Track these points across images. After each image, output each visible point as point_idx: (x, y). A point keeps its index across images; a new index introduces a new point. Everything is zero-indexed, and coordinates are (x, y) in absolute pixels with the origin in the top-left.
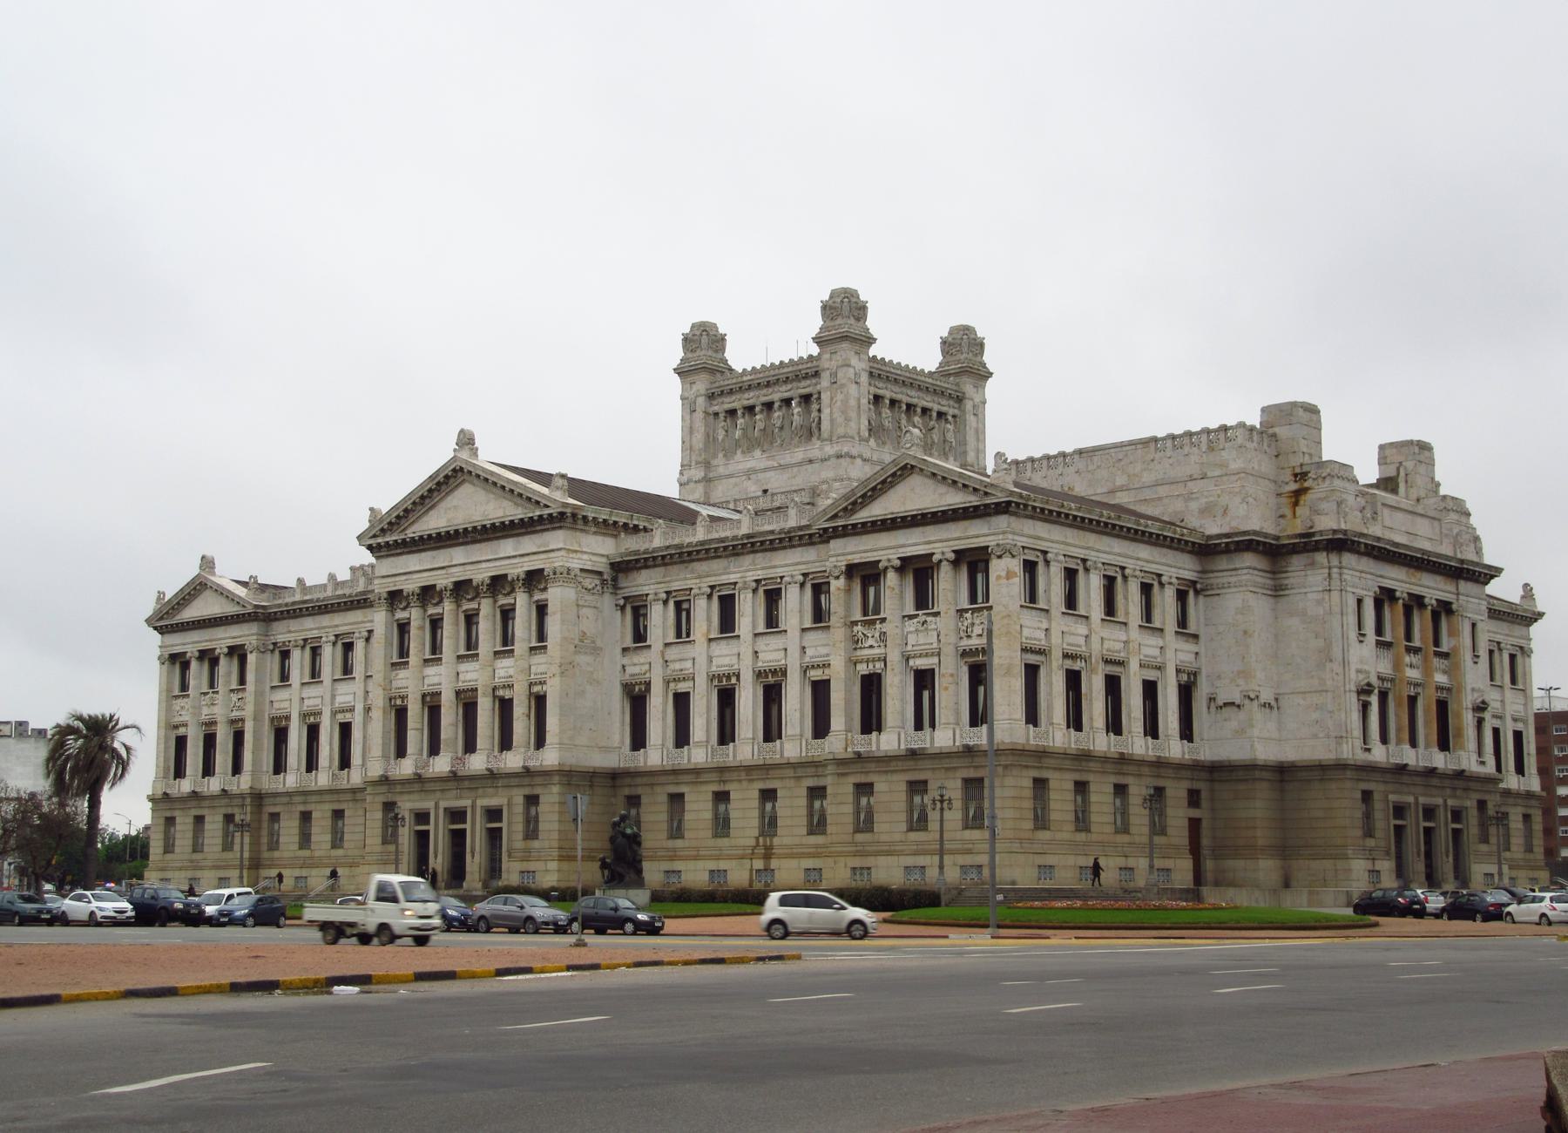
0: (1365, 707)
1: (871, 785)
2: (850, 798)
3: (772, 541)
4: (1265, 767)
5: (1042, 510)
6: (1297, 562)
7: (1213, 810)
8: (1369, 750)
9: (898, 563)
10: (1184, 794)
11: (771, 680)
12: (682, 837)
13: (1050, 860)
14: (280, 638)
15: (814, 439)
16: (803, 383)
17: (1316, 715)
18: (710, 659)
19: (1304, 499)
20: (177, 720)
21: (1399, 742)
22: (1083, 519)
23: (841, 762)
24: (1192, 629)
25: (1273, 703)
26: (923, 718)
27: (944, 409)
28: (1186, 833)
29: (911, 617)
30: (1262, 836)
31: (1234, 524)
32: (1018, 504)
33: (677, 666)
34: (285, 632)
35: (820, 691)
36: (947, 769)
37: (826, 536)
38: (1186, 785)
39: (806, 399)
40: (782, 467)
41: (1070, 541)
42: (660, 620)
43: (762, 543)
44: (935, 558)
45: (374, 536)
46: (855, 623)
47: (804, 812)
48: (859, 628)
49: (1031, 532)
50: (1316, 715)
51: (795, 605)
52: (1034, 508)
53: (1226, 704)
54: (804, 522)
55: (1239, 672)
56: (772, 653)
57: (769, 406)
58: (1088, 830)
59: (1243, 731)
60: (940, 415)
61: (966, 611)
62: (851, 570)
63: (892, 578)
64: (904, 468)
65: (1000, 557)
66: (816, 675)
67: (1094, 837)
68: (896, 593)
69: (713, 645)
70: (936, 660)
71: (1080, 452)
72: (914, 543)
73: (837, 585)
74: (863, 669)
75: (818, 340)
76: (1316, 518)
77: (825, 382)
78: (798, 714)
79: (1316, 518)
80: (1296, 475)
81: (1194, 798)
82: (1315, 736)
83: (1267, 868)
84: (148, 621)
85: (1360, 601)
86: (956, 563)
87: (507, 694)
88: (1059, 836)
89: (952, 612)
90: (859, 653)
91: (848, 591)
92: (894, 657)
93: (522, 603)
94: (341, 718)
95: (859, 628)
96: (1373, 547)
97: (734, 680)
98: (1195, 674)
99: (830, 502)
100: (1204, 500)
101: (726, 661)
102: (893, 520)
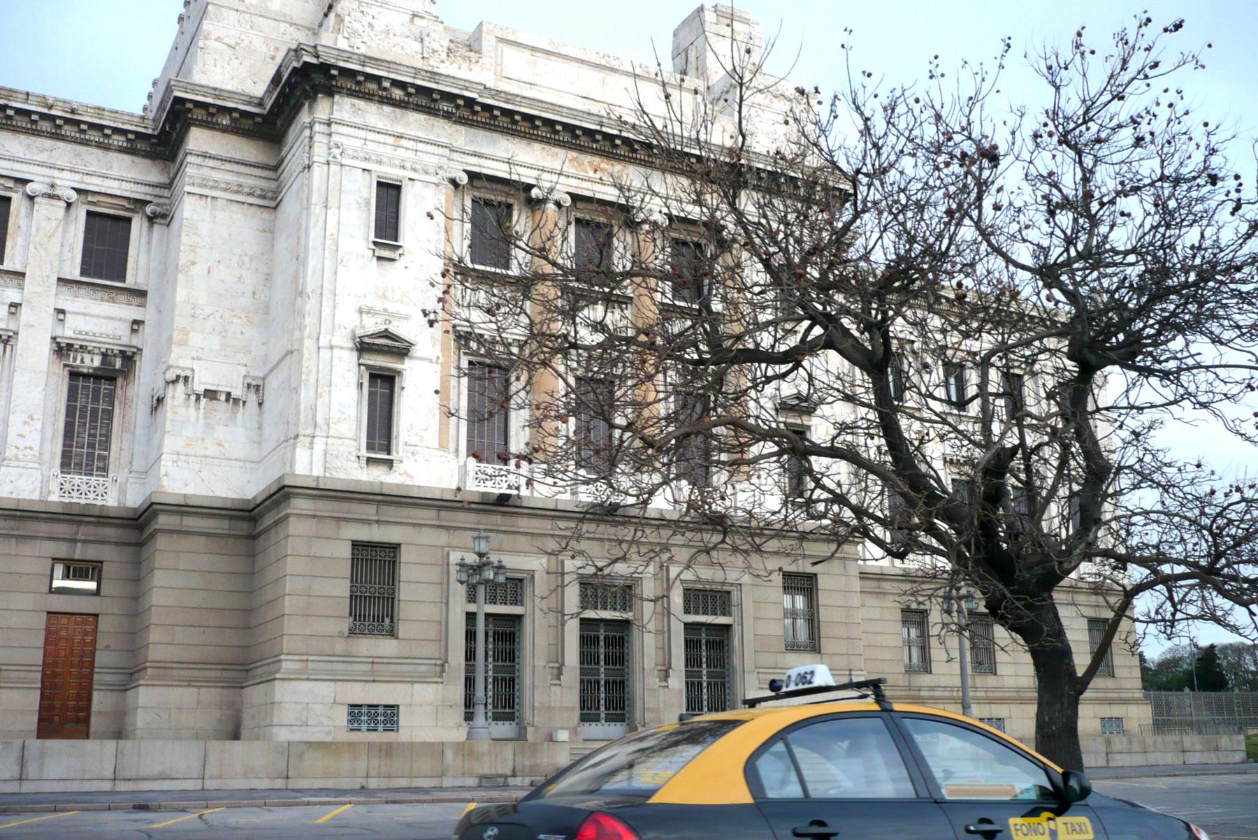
25: (236, 393)
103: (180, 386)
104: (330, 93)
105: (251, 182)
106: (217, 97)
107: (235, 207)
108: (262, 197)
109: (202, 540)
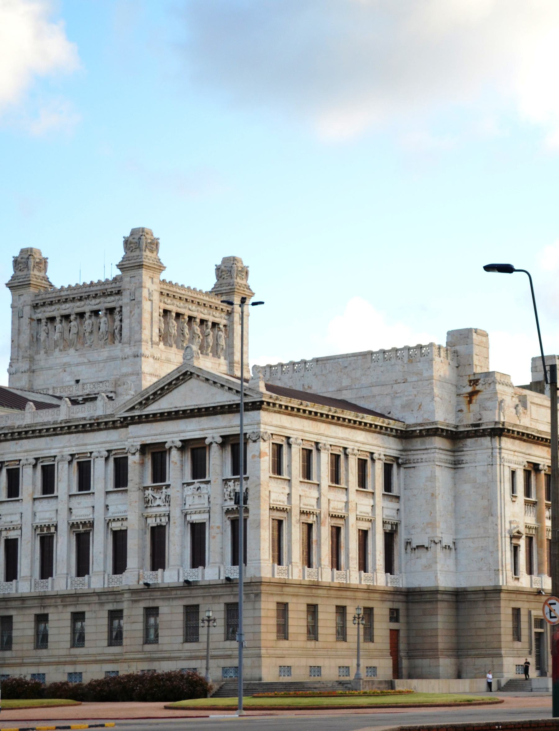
0: (516, 549)
1: (157, 608)
2: (141, 619)
3: (84, 426)
4: (445, 592)
5: (287, 407)
6: (469, 441)
7: (408, 623)
8: (518, 579)
10: (387, 612)
13: (287, 662)
15: (117, 342)
17: (481, 554)
19: (475, 398)
21: (540, 573)
22: (316, 413)
23: (133, 592)
24: (395, 492)
25: (452, 546)
26: (198, 558)
27: (217, 320)
28: (388, 640)
29: (189, 484)
30: (443, 641)
31: (426, 416)
32: (268, 403)
35: (119, 539)
36: (214, 597)
37: (126, 423)
38: (389, 605)
39: (111, 311)
40: (91, 363)
41: (306, 429)
43: (77, 426)
44: (207, 442)
46: (146, 488)
47: (106, 629)
49: (279, 423)
50: (481, 554)
51: (102, 474)
52: (280, 406)
53: (418, 547)
54: (109, 412)
55: (428, 524)
56: (82, 509)
57: (81, 315)
58: (316, 639)
59: (430, 566)
60: (214, 324)
61: (229, 480)
62: (144, 449)
63: (175, 455)
64: (185, 374)
65: (255, 441)
66: (117, 526)
67: (319, 644)
68: (177, 466)
70: (206, 516)
71: (317, 360)
72: (192, 429)
73: (133, 460)
74: (152, 522)
75: (120, 266)
76: (483, 413)
78: (102, 556)
79: (483, 413)
80: (470, 381)
81: (394, 615)
82: (480, 569)
83: (445, 664)
85: (513, 473)
86: (222, 445)
88: (295, 644)
89: (220, 481)
90: (149, 510)
91: (142, 464)
92: (176, 514)
95: (149, 492)
96: (523, 434)
98: (397, 525)
99: (129, 397)
100: (405, 399)
102: (177, 412)
103: (439, 544)
104: (500, 436)
105: (449, 458)
106: (448, 426)
107: (446, 469)
108: (451, 464)
109: (446, 603)
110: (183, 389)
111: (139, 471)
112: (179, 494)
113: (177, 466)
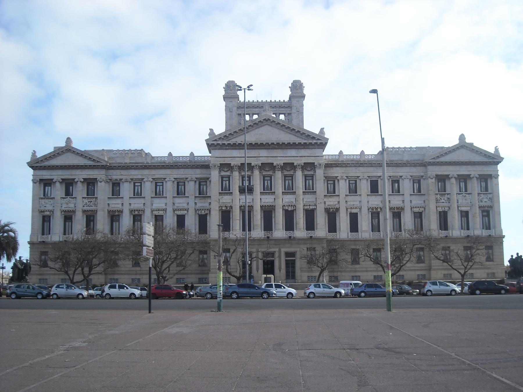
9: (457, 176)
11: (396, 210)
12: (359, 264)
14: (114, 177)
16: (281, 109)
18: (368, 202)
20: (42, 208)
33: (352, 203)
34: (116, 175)
42: (343, 187)
44: (471, 176)
45: (216, 140)
46: (437, 194)
48: (439, 196)
61: (481, 194)
69: (369, 197)
74: (440, 209)
77: (294, 110)
84: (28, 163)
87: (290, 209)
93: (299, 175)
94: (156, 213)
95: (439, 196)
97: (379, 210)
101: (376, 203)
110: (458, 152)
111: (430, 185)
112: (456, 198)
113: (452, 187)
